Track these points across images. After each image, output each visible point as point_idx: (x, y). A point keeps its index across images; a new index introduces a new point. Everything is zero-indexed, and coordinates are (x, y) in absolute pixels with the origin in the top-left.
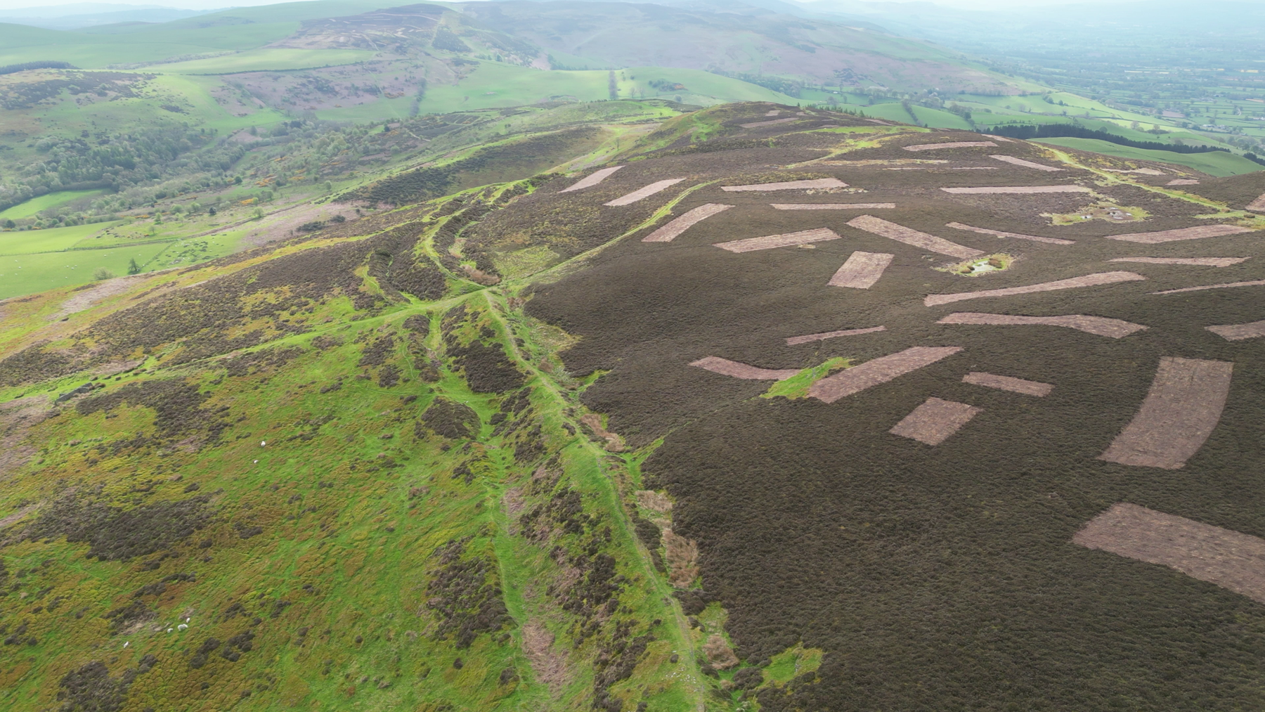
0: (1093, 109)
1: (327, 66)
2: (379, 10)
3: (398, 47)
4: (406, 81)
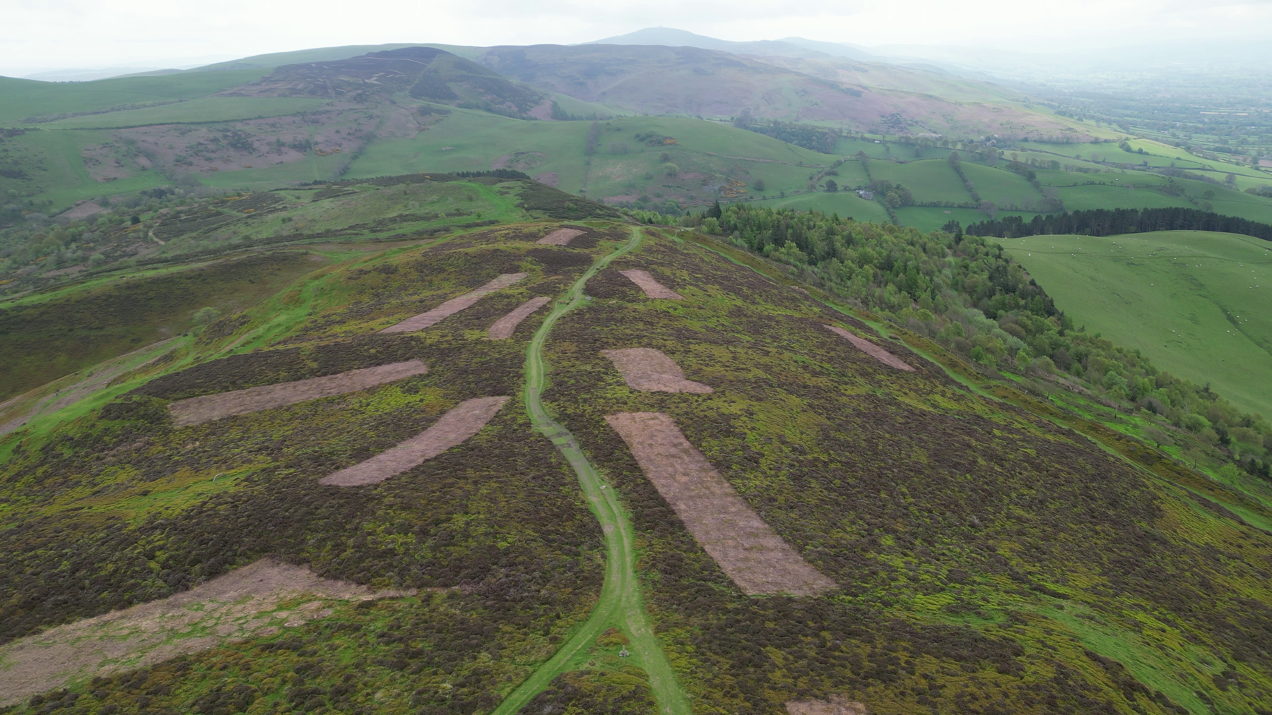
0: (1178, 158)
1: (260, 117)
2: (368, 55)
3: (358, 95)
4: (349, 134)
